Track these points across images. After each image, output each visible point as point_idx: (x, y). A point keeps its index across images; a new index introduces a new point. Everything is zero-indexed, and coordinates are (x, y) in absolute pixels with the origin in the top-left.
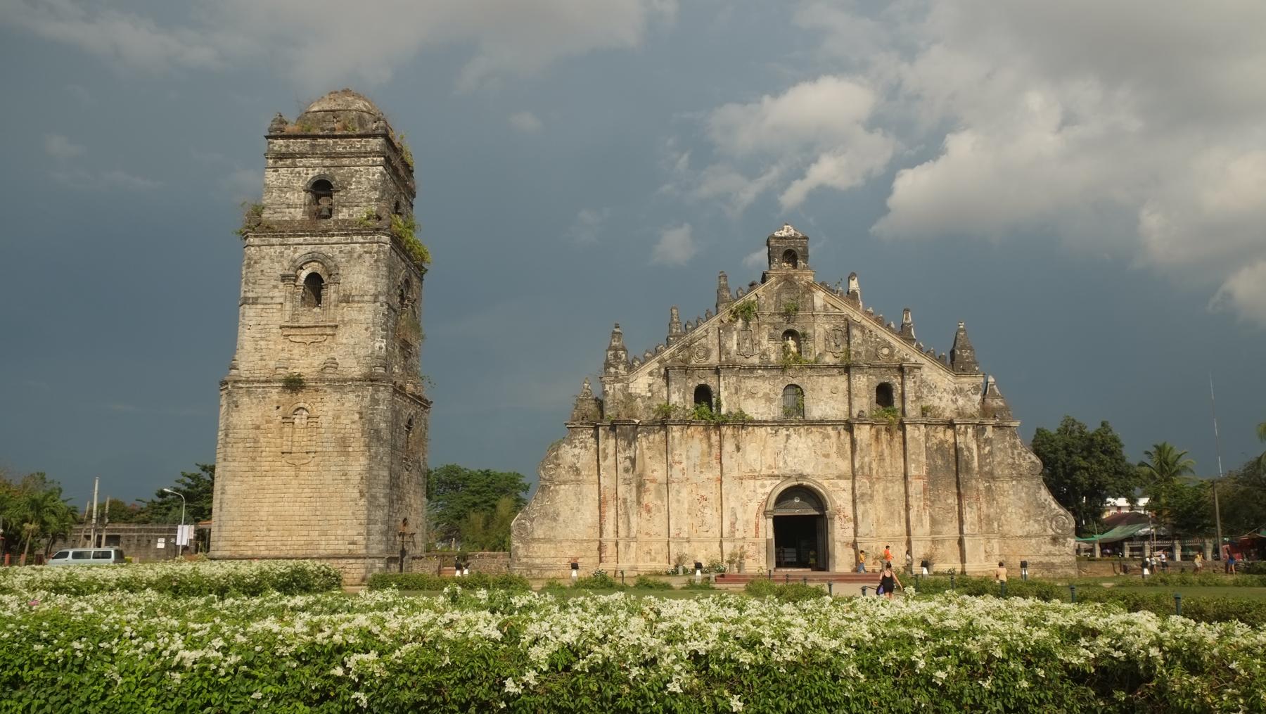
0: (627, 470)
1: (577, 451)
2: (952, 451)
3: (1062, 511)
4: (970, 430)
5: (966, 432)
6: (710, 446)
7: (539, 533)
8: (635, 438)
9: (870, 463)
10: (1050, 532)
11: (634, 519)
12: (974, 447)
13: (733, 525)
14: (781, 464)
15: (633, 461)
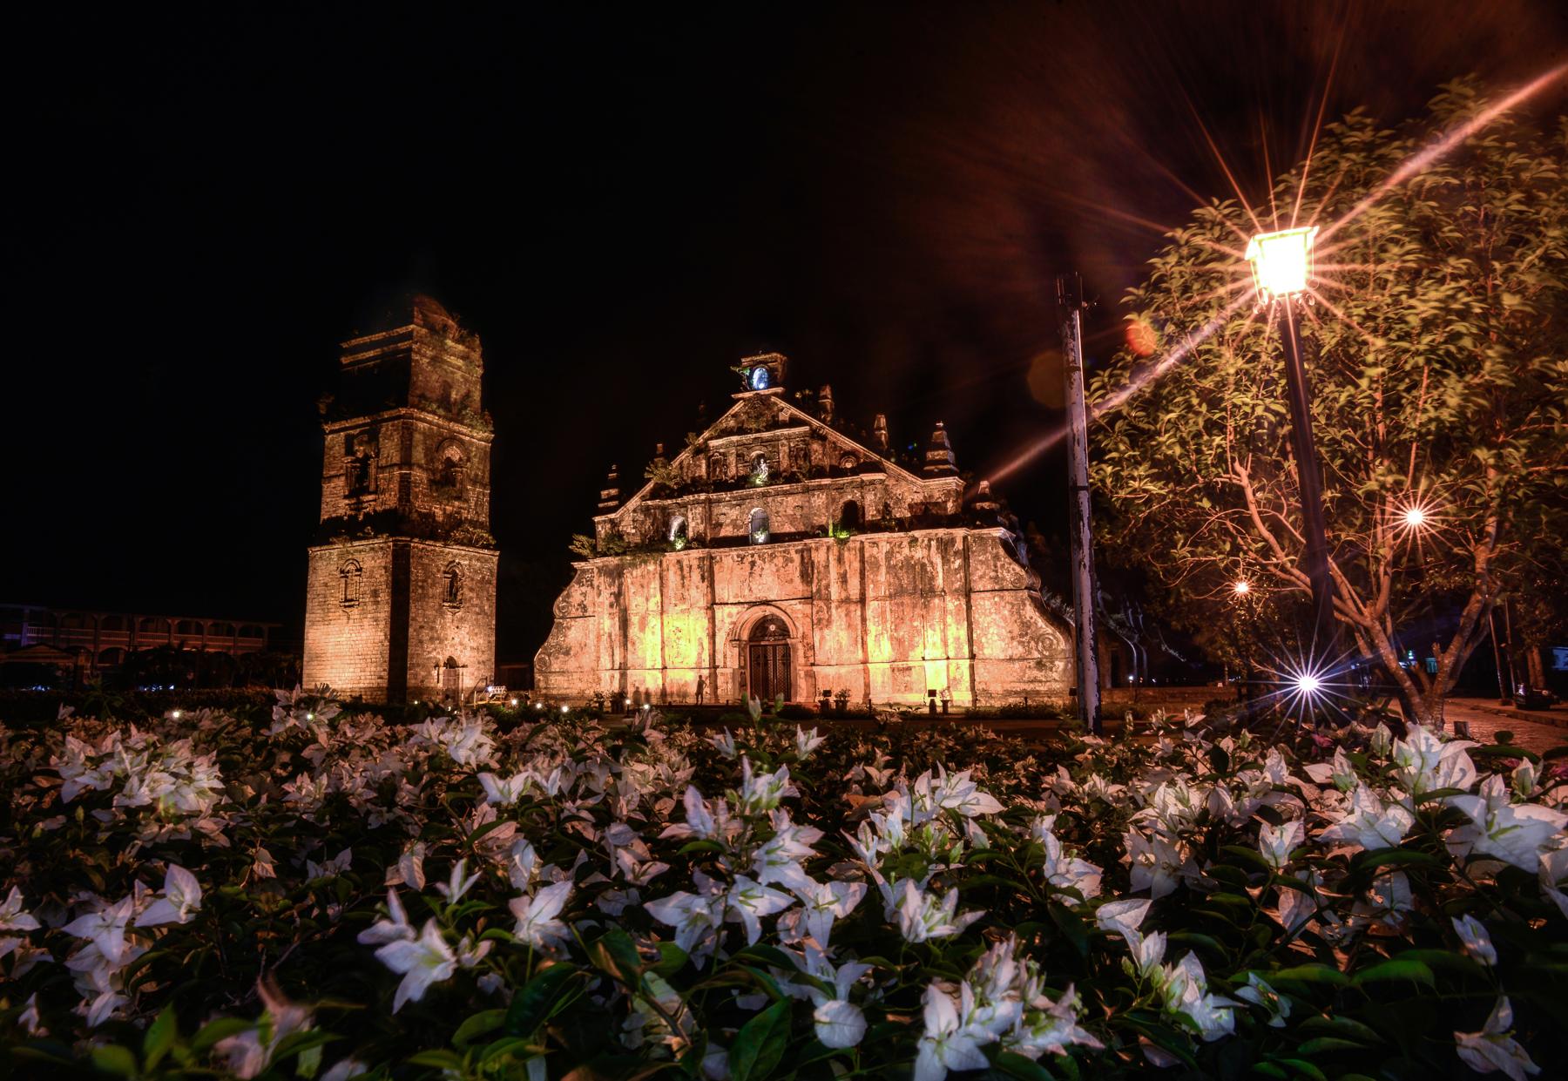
0: (611, 606)
1: (584, 589)
2: (918, 568)
3: (1050, 630)
4: (933, 543)
5: (929, 546)
6: (683, 577)
7: (555, 667)
8: (620, 575)
9: (828, 586)
10: (1036, 655)
11: (617, 651)
12: (938, 560)
13: (700, 655)
14: (747, 592)
15: (618, 595)
